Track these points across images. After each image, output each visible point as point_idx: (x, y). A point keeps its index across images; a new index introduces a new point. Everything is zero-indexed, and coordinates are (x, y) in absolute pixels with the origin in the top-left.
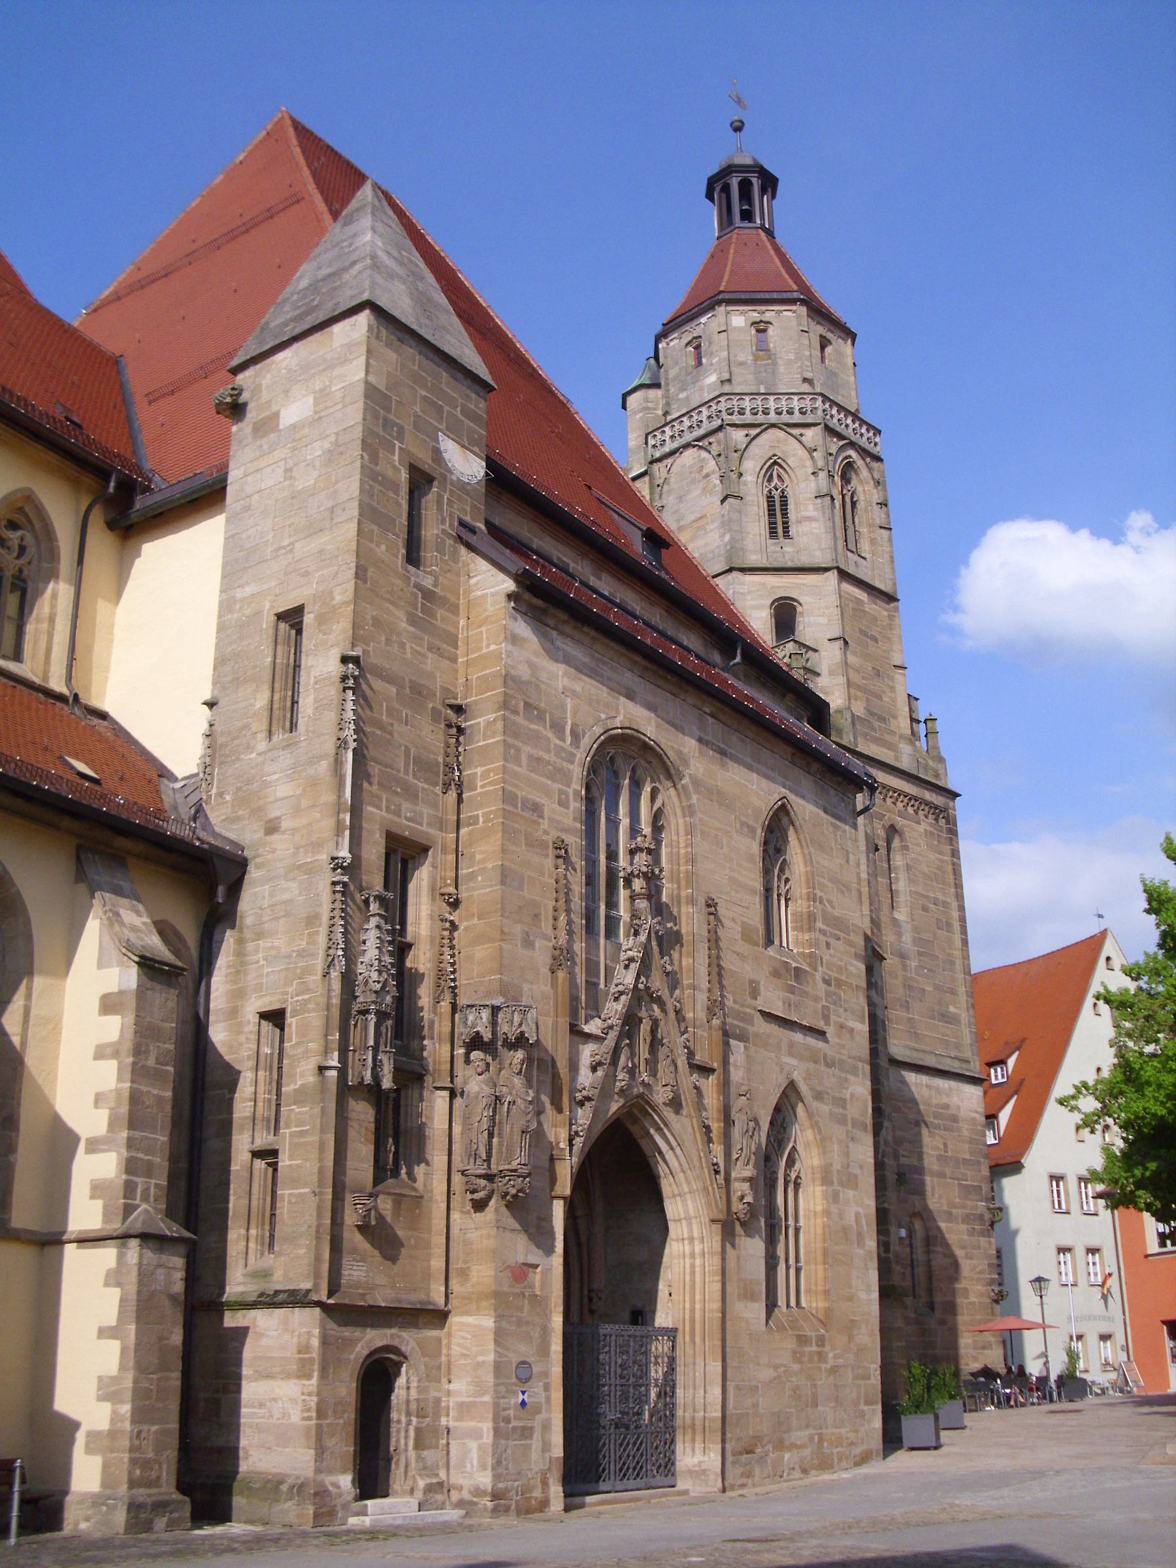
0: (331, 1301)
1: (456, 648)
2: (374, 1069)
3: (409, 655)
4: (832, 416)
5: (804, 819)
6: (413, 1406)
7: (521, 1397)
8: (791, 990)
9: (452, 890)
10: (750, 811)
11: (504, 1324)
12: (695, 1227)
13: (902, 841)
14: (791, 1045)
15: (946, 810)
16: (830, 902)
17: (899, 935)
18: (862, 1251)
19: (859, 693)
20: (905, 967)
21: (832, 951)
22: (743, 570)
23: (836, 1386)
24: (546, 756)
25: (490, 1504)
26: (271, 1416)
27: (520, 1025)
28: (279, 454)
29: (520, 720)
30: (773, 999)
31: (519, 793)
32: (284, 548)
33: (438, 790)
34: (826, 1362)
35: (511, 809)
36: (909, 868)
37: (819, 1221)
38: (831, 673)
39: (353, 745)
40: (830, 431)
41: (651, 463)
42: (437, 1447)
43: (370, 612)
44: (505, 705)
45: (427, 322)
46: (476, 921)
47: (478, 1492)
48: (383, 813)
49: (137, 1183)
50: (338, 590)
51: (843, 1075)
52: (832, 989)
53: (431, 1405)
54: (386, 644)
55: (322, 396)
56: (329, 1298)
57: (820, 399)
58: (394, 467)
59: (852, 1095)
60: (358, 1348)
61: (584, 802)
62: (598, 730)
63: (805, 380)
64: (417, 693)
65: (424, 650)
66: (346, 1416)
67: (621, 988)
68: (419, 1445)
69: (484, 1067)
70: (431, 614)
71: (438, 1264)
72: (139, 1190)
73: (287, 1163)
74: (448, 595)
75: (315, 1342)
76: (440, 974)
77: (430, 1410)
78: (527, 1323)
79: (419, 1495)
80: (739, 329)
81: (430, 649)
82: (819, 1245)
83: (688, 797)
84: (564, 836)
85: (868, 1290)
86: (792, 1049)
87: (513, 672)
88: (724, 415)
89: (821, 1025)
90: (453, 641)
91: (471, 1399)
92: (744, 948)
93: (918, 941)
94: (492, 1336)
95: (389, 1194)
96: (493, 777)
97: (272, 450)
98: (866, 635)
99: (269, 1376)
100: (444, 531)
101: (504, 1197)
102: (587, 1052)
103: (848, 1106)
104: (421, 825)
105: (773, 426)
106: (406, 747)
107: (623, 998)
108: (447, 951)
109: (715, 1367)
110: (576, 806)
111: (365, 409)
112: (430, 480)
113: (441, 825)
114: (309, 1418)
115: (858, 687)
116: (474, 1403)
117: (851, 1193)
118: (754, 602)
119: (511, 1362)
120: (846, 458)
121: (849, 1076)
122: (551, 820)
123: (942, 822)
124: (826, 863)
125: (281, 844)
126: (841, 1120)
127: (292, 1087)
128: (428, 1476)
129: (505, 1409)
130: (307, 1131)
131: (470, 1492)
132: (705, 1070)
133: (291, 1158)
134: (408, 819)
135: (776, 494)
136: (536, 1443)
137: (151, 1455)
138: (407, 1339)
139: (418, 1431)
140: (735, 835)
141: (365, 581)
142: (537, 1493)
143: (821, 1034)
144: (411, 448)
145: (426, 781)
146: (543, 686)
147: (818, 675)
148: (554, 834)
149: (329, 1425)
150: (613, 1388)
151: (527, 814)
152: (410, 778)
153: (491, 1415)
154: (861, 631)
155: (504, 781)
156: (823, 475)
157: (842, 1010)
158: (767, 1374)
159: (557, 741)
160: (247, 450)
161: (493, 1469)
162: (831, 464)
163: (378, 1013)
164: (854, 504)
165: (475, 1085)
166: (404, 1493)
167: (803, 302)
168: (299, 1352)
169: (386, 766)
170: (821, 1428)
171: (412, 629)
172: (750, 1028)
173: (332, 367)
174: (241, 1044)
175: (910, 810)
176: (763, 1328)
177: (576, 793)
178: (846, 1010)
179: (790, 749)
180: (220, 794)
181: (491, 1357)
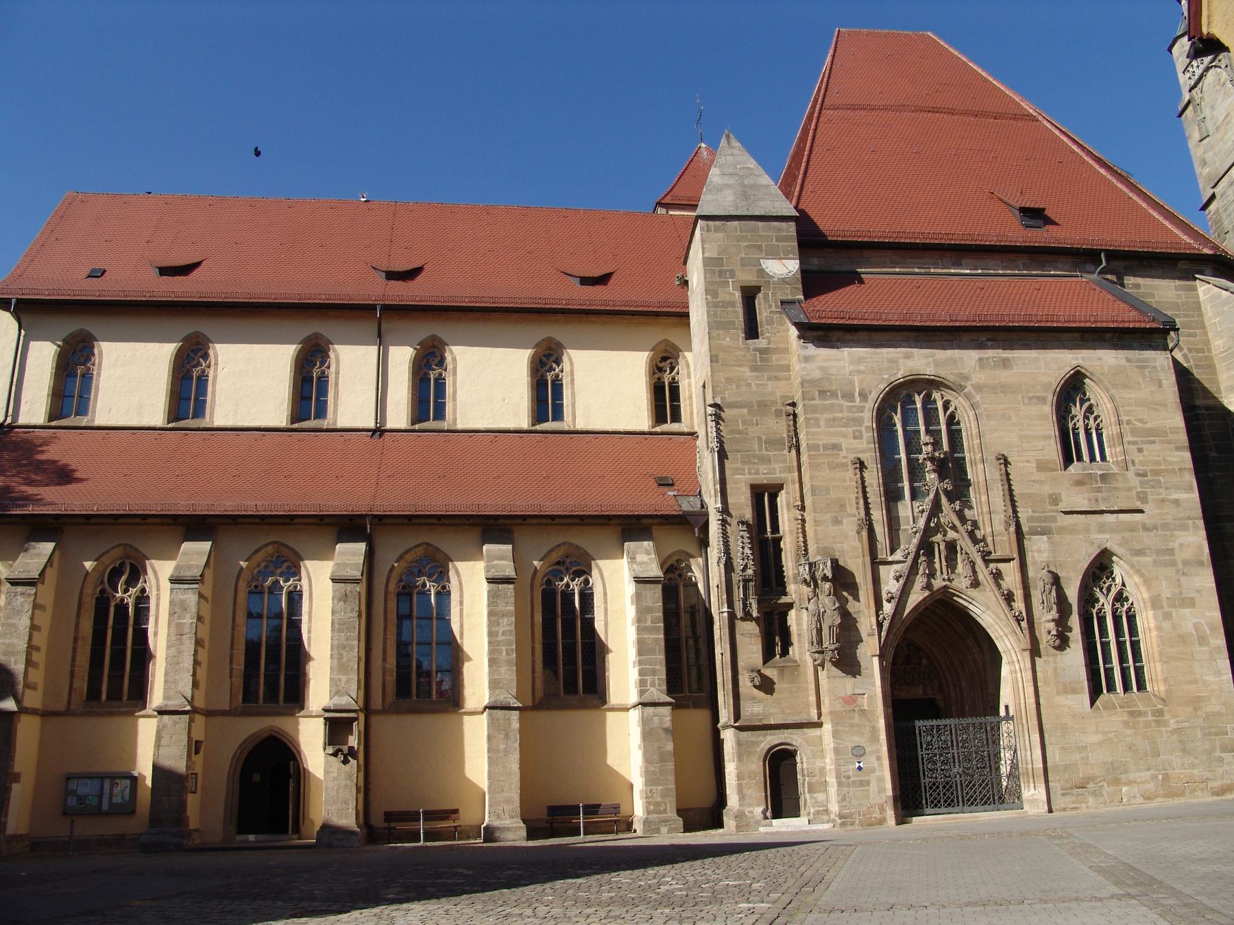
3: (754, 388)
7: (857, 765)
8: (1099, 490)
9: (799, 503)
11: (840, 728)
16: (1141, 421)
18: (1205, 648)
21: (1145, 453)
23: (1180, 741)
33: (786, 452)
43: (721, 377)
51: (1168, 533)
53: (817, 770)
54: (737, 388)
58: (730, 293)
59: (1181, 545)
60: (763, 744)
62: (882, 387)
68: (809, 792)
70: (767, 360)
74: (779, 346)
86: (1102, 528)
87: (808, 378)
89: (1138, 505)
106: (758, 437)
108: (801, 535)
109: (1036, 737)
111: (705, 273)
112: (757, 289)
119: (848, 747)
124: (1132, 396)
126: (1173, 563)
132: (1008, 560)
134: (763, 474)
136: (873, 787)
138: (794, 738)
141: (717, 361)
142: (877, 815)
144: (740, 278)
145: (775, 450)
152: (764, 452)
163: (743, 580)
166: (804, 815)
169: (746, 451)
172: (1053, 525)
177: (867, 428)
178: (1167, 489)
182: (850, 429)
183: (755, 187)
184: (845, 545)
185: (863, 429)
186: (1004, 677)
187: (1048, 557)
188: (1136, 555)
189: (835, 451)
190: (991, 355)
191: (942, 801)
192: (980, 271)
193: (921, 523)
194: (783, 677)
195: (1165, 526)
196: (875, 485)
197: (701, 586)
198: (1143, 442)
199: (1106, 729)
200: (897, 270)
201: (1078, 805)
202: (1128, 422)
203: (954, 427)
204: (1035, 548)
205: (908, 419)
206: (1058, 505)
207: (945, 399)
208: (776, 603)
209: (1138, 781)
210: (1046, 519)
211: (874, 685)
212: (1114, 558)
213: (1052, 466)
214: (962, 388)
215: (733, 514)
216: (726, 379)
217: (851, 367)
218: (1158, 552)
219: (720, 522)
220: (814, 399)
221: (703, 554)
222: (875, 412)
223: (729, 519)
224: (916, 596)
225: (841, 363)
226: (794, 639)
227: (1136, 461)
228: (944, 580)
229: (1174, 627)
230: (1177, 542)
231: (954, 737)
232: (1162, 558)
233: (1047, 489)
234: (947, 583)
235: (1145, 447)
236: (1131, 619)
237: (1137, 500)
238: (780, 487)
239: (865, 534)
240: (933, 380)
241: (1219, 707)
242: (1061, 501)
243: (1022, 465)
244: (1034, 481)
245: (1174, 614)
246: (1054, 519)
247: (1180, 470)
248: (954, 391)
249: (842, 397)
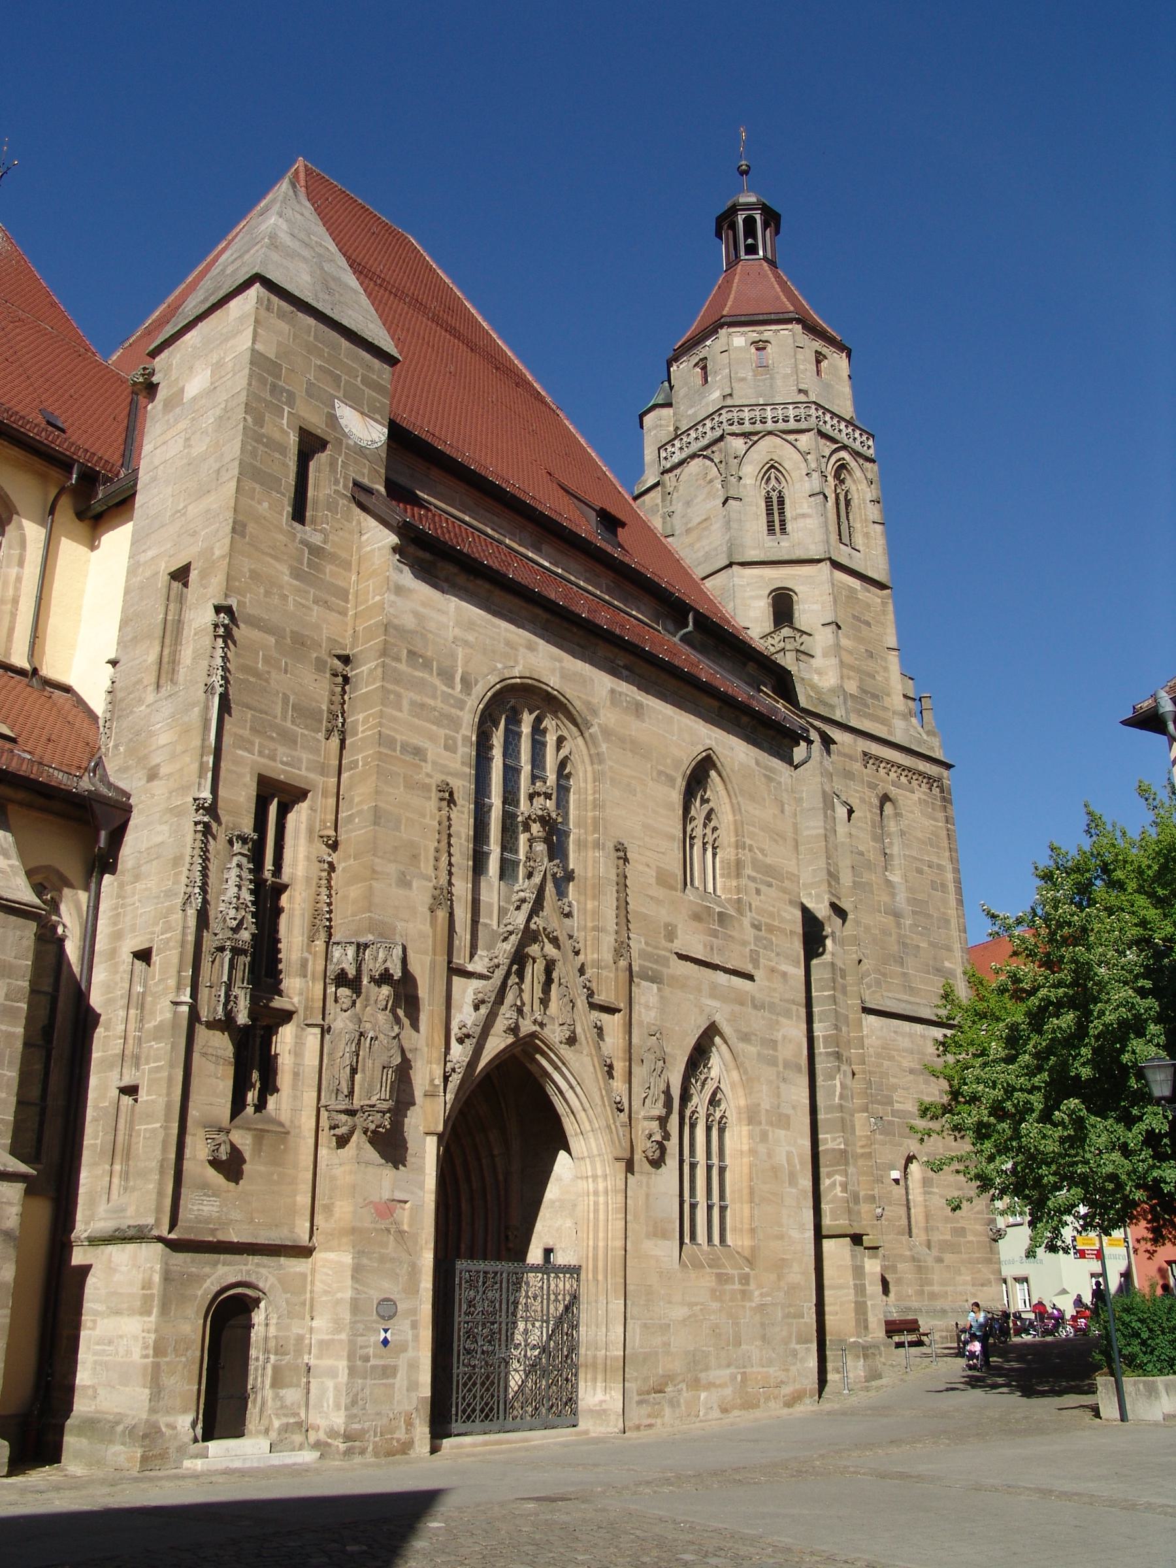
0: (172, 1236)
1: (347, 601)
2: (226, 1004)
3: (291, 607)
4: (825, 422)
5: (733, 771)
6: (272, 1344)
7: (383, 1335)
8: (714, 933)
9: (332, 833)
10: (669, 761)
11: (365, 1261)
12: (598, 1165)
13: (895, 808)
14: (714, 987)
15: (939, 780)
16: (762, 851)
17: (893, 895)
18: (794, 1190)
19: (852, 674)
20: (898, 925)
21: (762, 897)
22: (743, 564)
23: (762, 1325)
24: (431, 702)
25: (342, 1447)
26: (117, 1353)
27: (385, 961)
28: (182, 425)
29: (403, 667)
30: (694, 942)
31: (398, 737)
32: (179, 511)
33: (321, 736)
34: (751, 1300)
35: (389, 752)
36: (902, 833)
37: (746, 1160)
38: (825, 655)
39: (219, 690)
40: (822, 434)
41: (662, 473)
42: (298, 1386)
43: (246, 565)
44: (384, 653)
45: (327, 297)
46: (352, 861)
47: (332, 1433)
48: (255, 757)
50: (218, 544)
51: (774, 1017)
52: (763, 933)
53: (292, 1342)
54: (265, 596)
55: (218, 366)
56: (169, 1232)
57: (814, 407)
59: (784, 1037)
61: (475, 747)
62: (493, 679)
63: (800, 391)
64: (299, 644)
65: (310, 603)
66: (189, 1353)
67: (510, 928)
68: (275, 1384)
69: (350, 1003)
71: (304, 1200)
73: (145, 1098)
75: (157, 1278)
76: (316, 914)
77: (292, 1348)
78: (392, 1260)
79: (273, 1435)
80: (740, 348)
81: (316, 602)
82: (745, 1184)
83: (596, 745)
84: (450, 780)
85: (802, 1228)
87: (396, 621)
88: (725, 426)
89: (748, 968)
90: (344, 594)
91: (330, 1337)
92: (660, 893)
93: (912, 901)
94: (349, 1273)
95: (249, 1129)
96: (372, 721)
97: (177, 421)
98: (859, 620)
99: (117, 1312)
100: (336, 492)
101: (365, 1133)
102: (466, 991)
104: (300, 769)
105: (770, 433)
107: (513, 937)
108: (324, 891)
110: (466, 752)
112: (322, 445)
113: (323, 770)
114: (146, 1356)
115: (851, 668)
116: (333, 1340)
117: (782, 1132)
118: (753, 593)
120: (839, 460)
121: (781, 1019)
122: (434, 763)
123: (936, 791)
124: (757, 813)
125: (159, 788)
126: (773, 1062)
127: (153, 1023)
128: (285, 1415)
129: (361, 1347)
130: (161, 1067)
131: (326, 1433)
132: (611, 1010)
133: (148, 1094)
134: (283, 763)
135: (774, 495)
136: (400, 1380)
139: (276, 1369)
140: (651, 783)
141: (243, 536)
142: (401, 1434)
143: (750, 977)
144: (302, 413)
145: (306, 727)
146: (430, 636)
147: (813, 657)
148: (438, 778)
149: (168, 1363)
150: (504, 1325)
151: (408, 758)
152: (289, 724)
153: (345, 1354)
154: (854, 617)
155: (380, 724)
156: (815, 475)
157: (773, 955)
158: (679, 1312)
159: (445, 688)
160: (157, 425)
161: (346, 1409)
162: (824, 466)
164: (848, 503)
165: (341, 1022)
166: (258, 1432)
167: (798, 321)
168: (143, 1288)
169: (261, 712)
170: (744, 1367)
172: (665, 971)
173: (227, 340)
174: (116, 984)
175: (903, 779)
176: (676, 1266)
177: (466, 739)
179: (716, 704)
180: (116, 746)
181: (348, 1294)
183: (337, 280)
184: (411, 925)
185: (459, 738)
186: (553, 1202)
191: (478, 1408)
192: (560, 571)
193: (520, 918)
194: (260, 1151)
195: (772, 1007)
197: (72, 949)
199: (693, 1300)
200: (467, 518)
201: (653, 1421)
203: (563, 782)
205: (511, 749)
207: (560, 733)
208: (267, 1006)
209: (718, 1382)
210: (658, 960)
211: (422, 1186)
212: (717, 1039)
214: (589, 725)
215: (224, 819)
216: (251, 571)
217: (457, 632)
219: (200, 827)
220: (398, 659)
221: (93, 886)
222: (478, 716)
223: (214, 825)
224: (497, 1043)
225: (444, 619)
226: (284, 1079)
227: (753, 906)
228: (535, 1022)
229: (770, 1156)
231: (504, 1296)
232: (766, 1052)
233: (663, 915)
234: (537, 1028)
238: (300, 794)
239: (442, 914)
240: (555, 697)
241: (799, 1276)
244: (652, 898)
246: (665, 962)
248: (576, 724)
249: (438, 674)
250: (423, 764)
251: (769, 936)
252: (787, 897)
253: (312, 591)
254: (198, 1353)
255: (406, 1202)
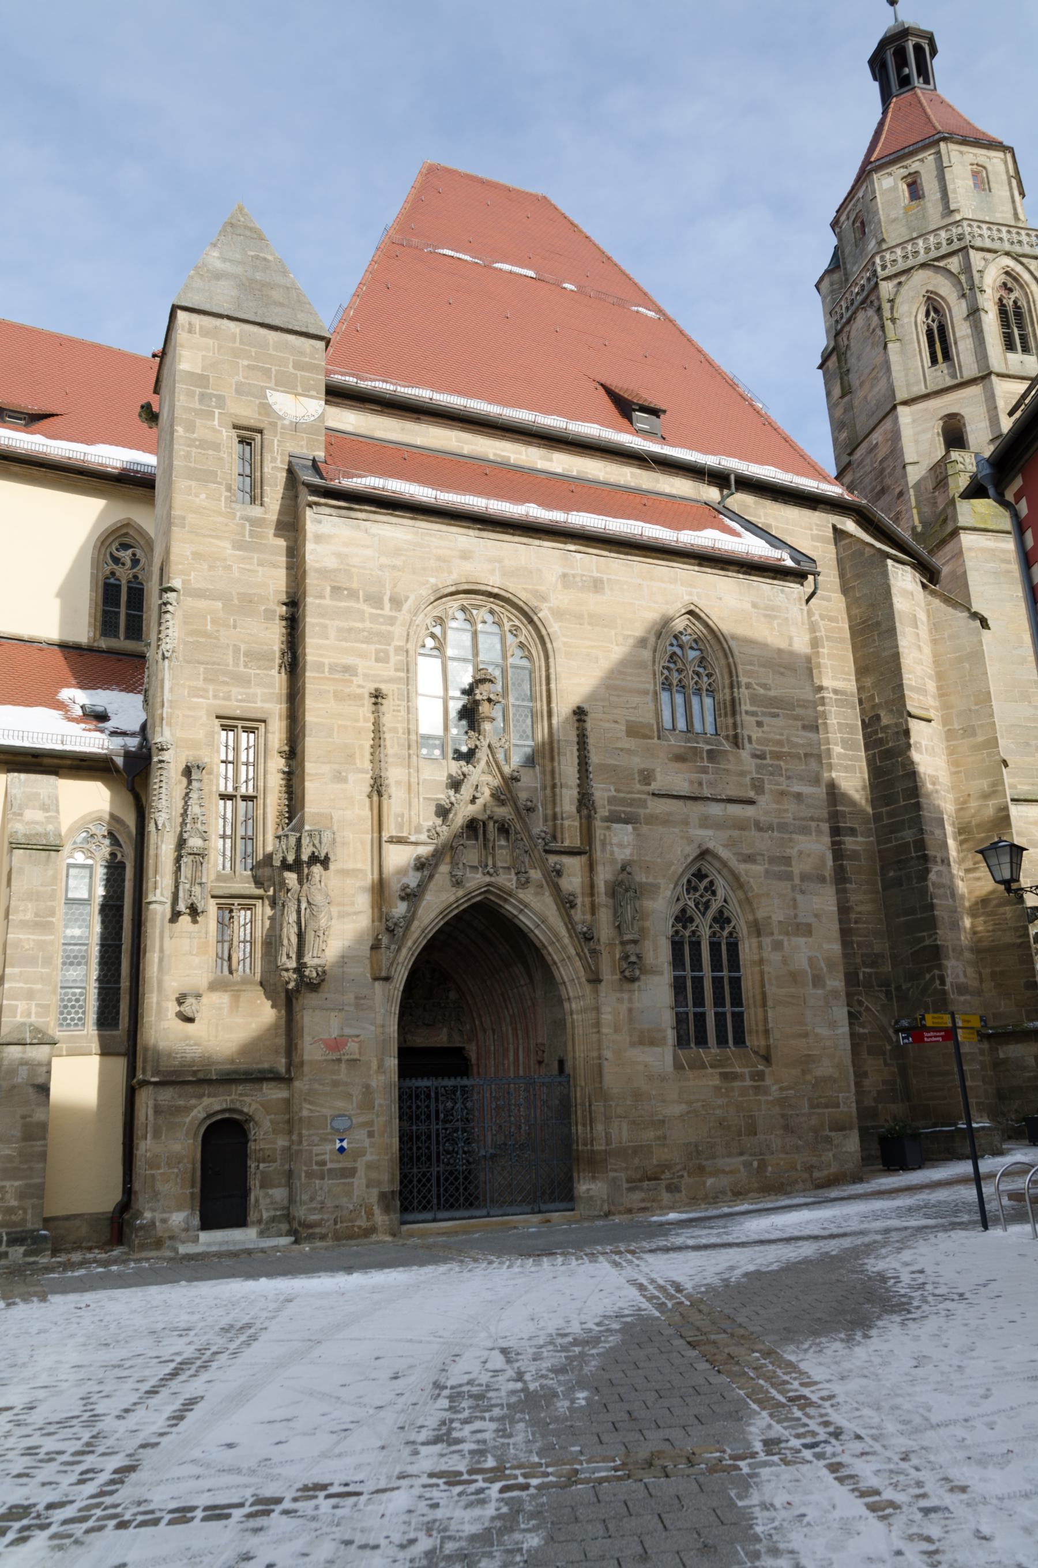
7: (338, 1145)
8: (704, 770)
11: (317, 1086)
16: (764, 686)
21: (765, 728)
48: (211, 701)
49: (17, 1006)
51: (786, 836)
52: (768, 761)
56: (153, 1076)
59: (800, 853)
60: (195, 1112)
66: (181, 1165)
68: (262, 1187)
72: (19, 1011)
86: (705, 822)
89: (752, 794)
95: (226, 991)
103: (794, 863)
119: (326, 1117)
121: (794, 836)
126: (788, 877)
135: (935, 326)
137: (14, 1203)
143: (751, 802)
145: (259, 668)
146: (354, 570)
149: (161, 1174)
169: (214, 663)
171: (237, 552)
172: (641, 811)
182: (373, 647)
187: (632, 855)
188: (745, 861)
189: (347, 676)
190: (580, 572)
195: (783, 827)
196: (401, 731)
198: (764, 714)
202: (748, 686)
204: (615, 840)
206: (650, 784)
210: (632, 803)
213: (647, 732)
216: (194, 553)
218: (772, 860)
220: (322, 597)
227: (754, 738)
230: (796, 850)
232: (776, 869)
233: (637, 762)
235: (766, 720)
236: (733, 947)
237: (752, 789)
242: (655, 780)
243: (606, 725)
244: (622, 750)
245: (786, 943)
246: (643, 804)
247: (806, 755)
250: (354, 678)
251: (776, 763)
252: (799, 723)
253: (256, 556)
254: (189, 1166)
255: (358, 1036)
